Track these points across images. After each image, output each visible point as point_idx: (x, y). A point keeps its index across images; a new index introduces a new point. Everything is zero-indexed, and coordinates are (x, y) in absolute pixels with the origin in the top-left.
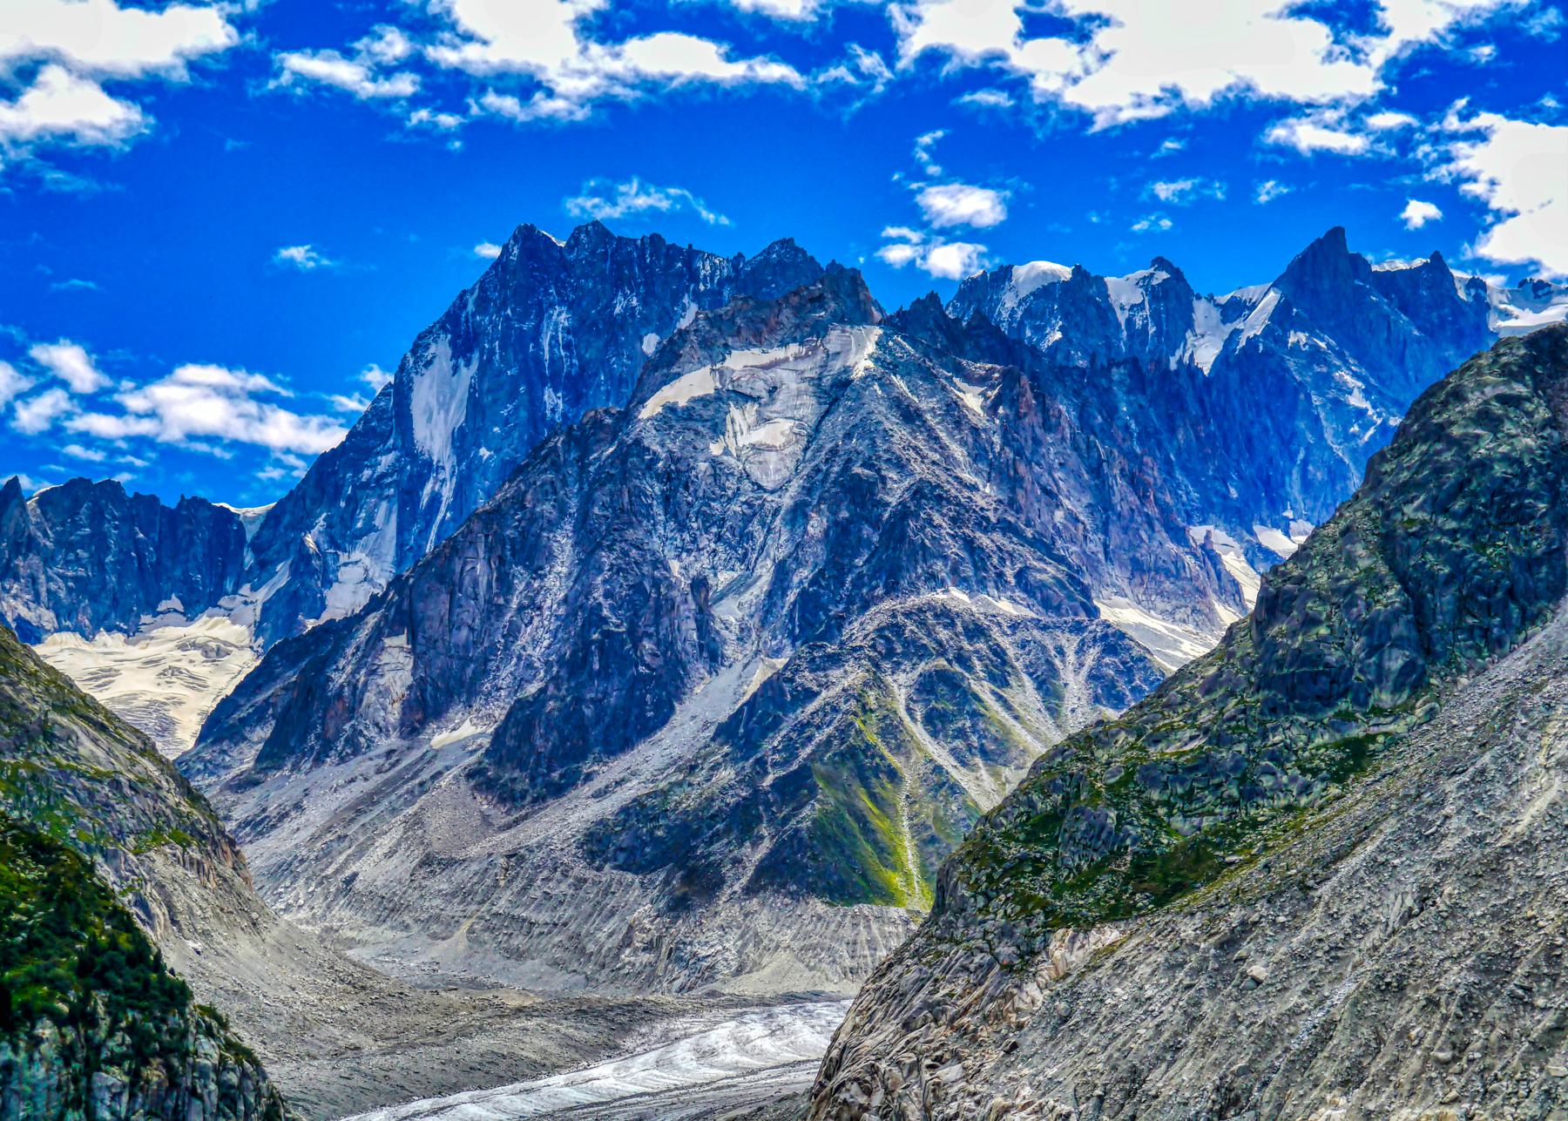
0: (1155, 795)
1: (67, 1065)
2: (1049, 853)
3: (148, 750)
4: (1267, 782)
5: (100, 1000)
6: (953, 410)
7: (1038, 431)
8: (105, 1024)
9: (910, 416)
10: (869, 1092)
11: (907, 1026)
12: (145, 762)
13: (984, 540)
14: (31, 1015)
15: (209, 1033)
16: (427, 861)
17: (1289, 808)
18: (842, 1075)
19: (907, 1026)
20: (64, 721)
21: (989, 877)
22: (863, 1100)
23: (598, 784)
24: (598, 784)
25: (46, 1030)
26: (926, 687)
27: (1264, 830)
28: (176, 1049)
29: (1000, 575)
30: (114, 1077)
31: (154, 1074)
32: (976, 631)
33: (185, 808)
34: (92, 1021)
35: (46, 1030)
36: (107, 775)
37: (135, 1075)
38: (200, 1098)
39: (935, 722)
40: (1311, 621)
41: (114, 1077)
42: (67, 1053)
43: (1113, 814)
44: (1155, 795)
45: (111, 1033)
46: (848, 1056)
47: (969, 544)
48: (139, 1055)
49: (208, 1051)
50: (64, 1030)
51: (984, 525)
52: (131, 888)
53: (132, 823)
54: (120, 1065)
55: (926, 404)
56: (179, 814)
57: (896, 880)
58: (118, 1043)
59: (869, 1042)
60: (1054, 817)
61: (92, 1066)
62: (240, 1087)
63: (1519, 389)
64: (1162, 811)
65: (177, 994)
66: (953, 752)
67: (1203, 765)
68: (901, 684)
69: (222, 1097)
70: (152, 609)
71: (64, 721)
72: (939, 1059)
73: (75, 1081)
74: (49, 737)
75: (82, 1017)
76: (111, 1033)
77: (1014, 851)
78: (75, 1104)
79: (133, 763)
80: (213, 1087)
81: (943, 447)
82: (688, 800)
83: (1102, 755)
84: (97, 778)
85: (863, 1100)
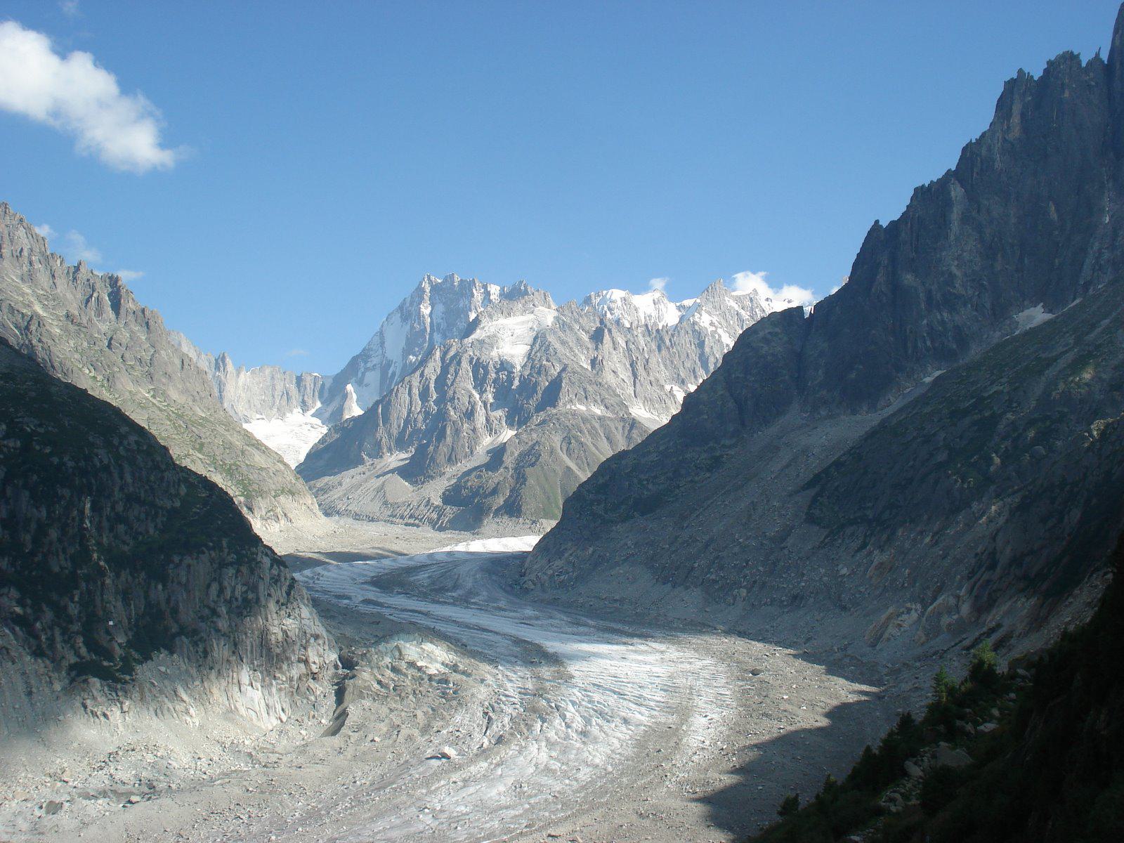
0: (642, 476)
1: (212, 565)
2: (603, 497)
3: (281, 461)
4: (683, 472)
5: (224, 543)
6: (578, 340)
7: (612, 350)
8: (226, 551)
9: (563, 343)
10: (535, 584)
11: (549, 561)
12: (279, 464)
13: (590, 388)
15: (267, 555)
16: (385, 503)
17: (692, 481)
18: (526, 578)
19: (549, 561)
20: (249, 449)
21: (581, 506)
22: (533, 587)
23: (447, 476)
24: (447, 476)
26: (567, 440)
27: (682, 489)
29: (596, 401)
30: (231, 571)
31: (244, 569)
32: (585, 420)
33: (293, 481)
34: (221, 549)
36: (265, 469)
37: (238, 571)
38: (263, 579)
39: (569, 453)
42: (212, 561)
43: (627, 483)
44: (642, 476)
45: (229, 554)
46: (528, 571)
47: (585, 390)
48: (239, 562)
49: (267, 561)
50: (211, 552)
51: (590, 382)
52: (272, 510)
53: (273, 487)
54: (232, 566)
55: (571, 340)
56: (291, 483)
59: (535, 567)
62: (279, 575)
63: (777, 330)
64: (645, 482)
65: (257, 540)
66: (577, 464)
68: (557, 440)
69: (271, 579)
70: (291, 411)
71: (249, 449)
72: (561, 572)
73: (215, 571)
74: (243, 452)
76: (229, 554)
78: (215, 579)
79: (274, 463)
80: (268, 575)
81: (575, 355)
83: (623, 462)
84: (262, 469)
85: (533, 587)
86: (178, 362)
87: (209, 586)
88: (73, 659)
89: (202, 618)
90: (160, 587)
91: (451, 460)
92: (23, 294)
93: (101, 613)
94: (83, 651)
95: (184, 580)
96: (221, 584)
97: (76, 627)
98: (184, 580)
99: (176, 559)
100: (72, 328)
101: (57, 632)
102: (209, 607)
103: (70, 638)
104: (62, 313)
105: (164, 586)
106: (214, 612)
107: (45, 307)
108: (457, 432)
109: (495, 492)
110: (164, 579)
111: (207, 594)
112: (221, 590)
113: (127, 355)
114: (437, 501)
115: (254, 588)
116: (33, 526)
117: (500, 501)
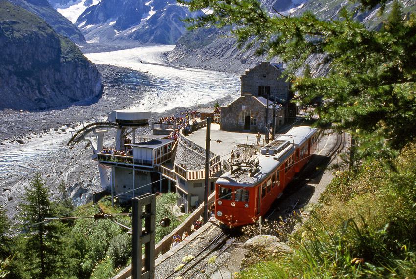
39: (176, 22)
57: (170, 41)
87: (73, 73)
88: (36, 98)
89: (72, 83)
90: (58, 74)
93: (42, 83)
94: (38, 95)
95: (65, 72)
96: (77, 73)
97: (35, 87)
98: (65, 72)
101: (30, 88)
102: (74, 80)
103: (34, 91)
105: (60, 73)
106: (76, 82)
110: (59, 71)
111: (73, 76)
112: (77, 75)
116: (18, 56)
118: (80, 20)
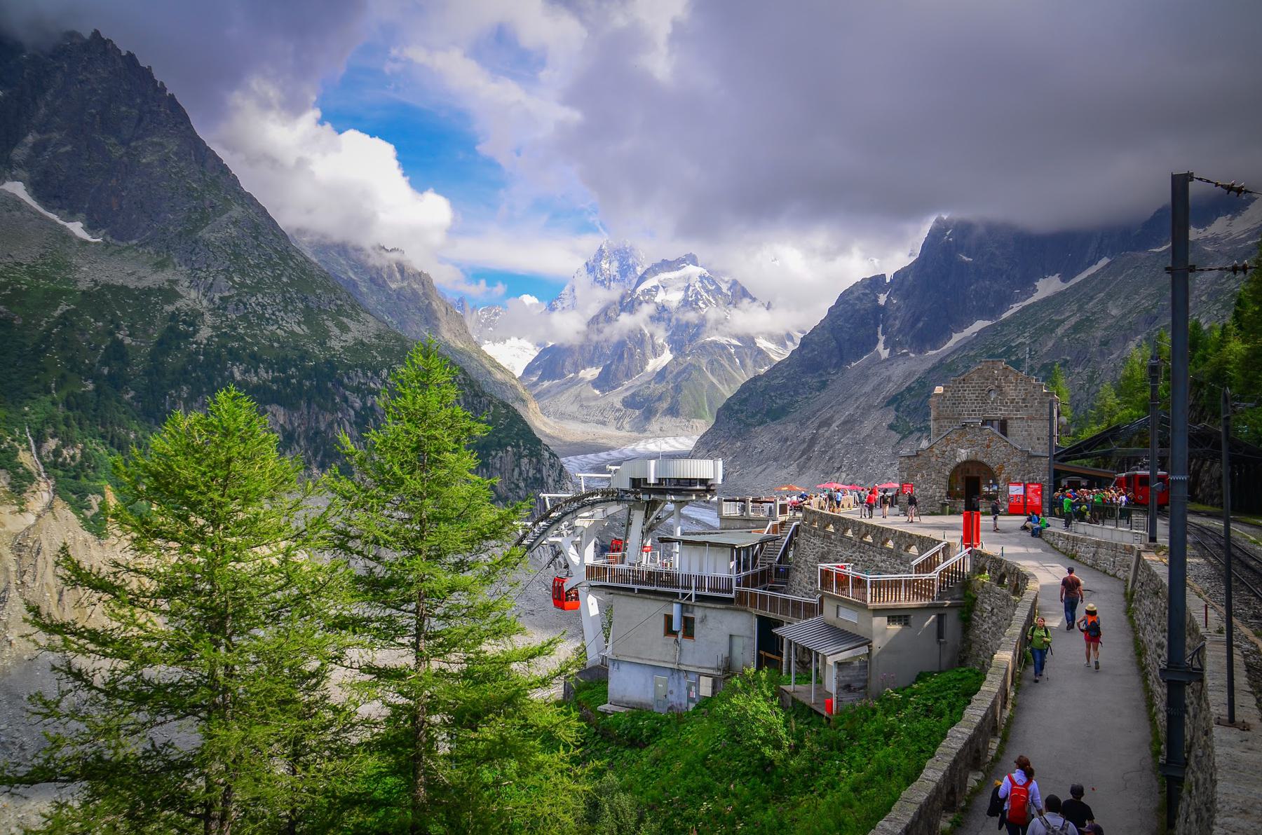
14: (506, 445)
25: (509, 449)
26: (711, 363)
28: (538, 456)
30: (525, 460)
31: (534, 460)
34: (519, 446)
35: (509, 449)
40: (813, 350)
41: (525, 460)
42: (515, 454)
49: (546, 454)
58: (526, 452)
60: (746, 400)
61: (521, 457)
67: (784, 385)
75: (518, 446)
77: (736, 407)
82: (648, 392)
86: (444, 310)
91: (628, 376)
92: (341, 265)
99: (493, 453)
100: (374, 288)
104: (367, 277)
106: (517, 486)
107: (355, 273)
108: (632, 355)
109: (660, 398)
113: (411, 306)
114: (619, 405)
115: (540, 471)
117: (665, 405)
118: (529, 370)
